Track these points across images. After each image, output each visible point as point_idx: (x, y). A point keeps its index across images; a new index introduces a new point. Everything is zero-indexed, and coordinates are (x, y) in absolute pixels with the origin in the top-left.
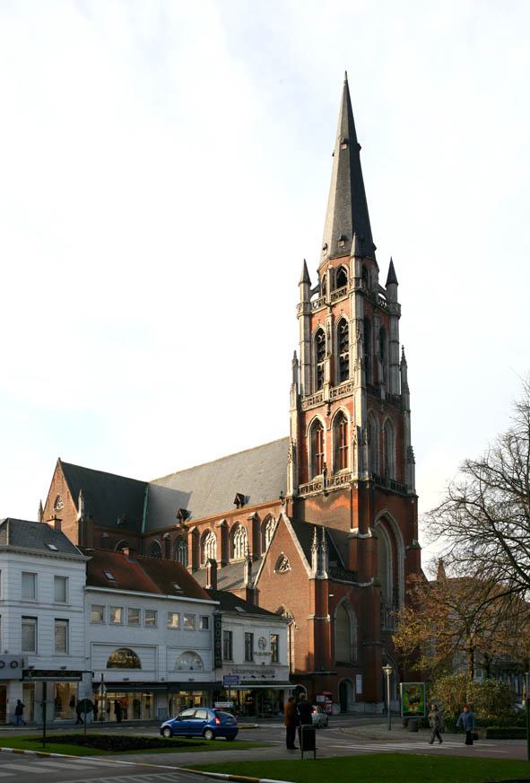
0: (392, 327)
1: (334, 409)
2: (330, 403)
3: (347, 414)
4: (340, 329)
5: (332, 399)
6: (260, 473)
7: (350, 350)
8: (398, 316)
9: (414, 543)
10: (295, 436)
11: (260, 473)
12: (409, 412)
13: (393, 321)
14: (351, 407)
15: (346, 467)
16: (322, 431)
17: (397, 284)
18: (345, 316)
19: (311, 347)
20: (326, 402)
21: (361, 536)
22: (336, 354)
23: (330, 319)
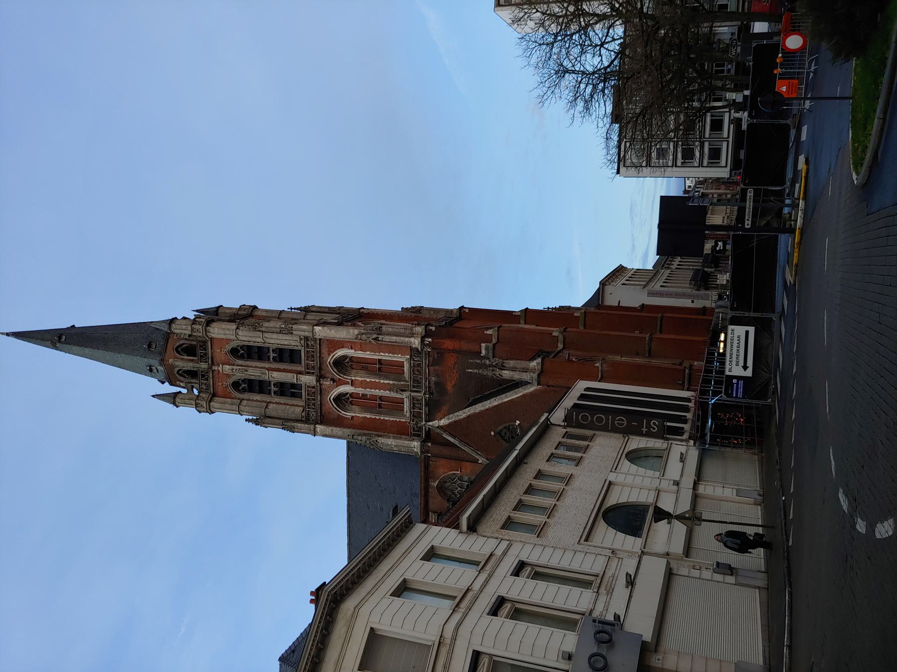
0: (264, 314)
1: (333, 372)
2: (320, 377)
3: (340, 353)
4: (242, 357)
5: (316, 371)
6: (382, 509)
7: (266, 345)
8: (255, 307)
9: (519, 314)
10: (347, 431)
11: (382, 509)
12: (363, 308)
13: (256, 313)
14: (336, 344)
15: (401, 365)
16: (352, 395)
17: (222, 306)
18: (228, 347)
19: (248, 400)
20: (318, 381)
21: (494, 341)
22: (267, 365)
23: (227, 367)
